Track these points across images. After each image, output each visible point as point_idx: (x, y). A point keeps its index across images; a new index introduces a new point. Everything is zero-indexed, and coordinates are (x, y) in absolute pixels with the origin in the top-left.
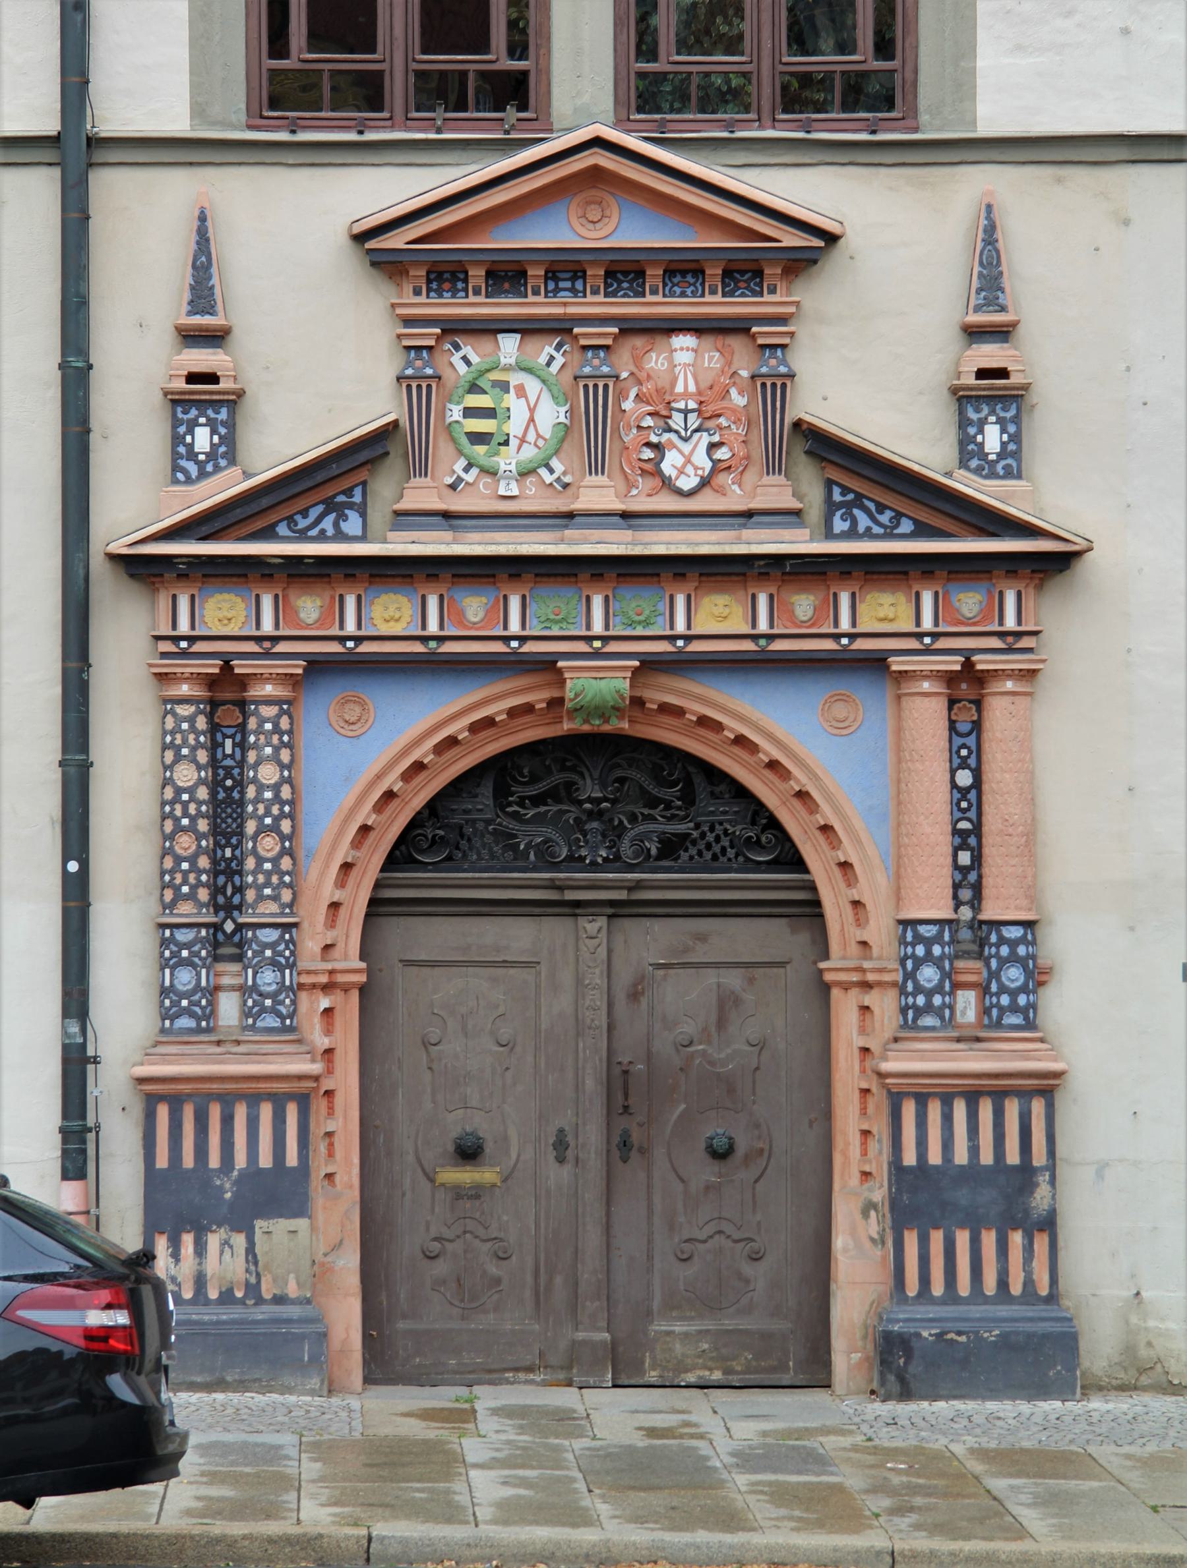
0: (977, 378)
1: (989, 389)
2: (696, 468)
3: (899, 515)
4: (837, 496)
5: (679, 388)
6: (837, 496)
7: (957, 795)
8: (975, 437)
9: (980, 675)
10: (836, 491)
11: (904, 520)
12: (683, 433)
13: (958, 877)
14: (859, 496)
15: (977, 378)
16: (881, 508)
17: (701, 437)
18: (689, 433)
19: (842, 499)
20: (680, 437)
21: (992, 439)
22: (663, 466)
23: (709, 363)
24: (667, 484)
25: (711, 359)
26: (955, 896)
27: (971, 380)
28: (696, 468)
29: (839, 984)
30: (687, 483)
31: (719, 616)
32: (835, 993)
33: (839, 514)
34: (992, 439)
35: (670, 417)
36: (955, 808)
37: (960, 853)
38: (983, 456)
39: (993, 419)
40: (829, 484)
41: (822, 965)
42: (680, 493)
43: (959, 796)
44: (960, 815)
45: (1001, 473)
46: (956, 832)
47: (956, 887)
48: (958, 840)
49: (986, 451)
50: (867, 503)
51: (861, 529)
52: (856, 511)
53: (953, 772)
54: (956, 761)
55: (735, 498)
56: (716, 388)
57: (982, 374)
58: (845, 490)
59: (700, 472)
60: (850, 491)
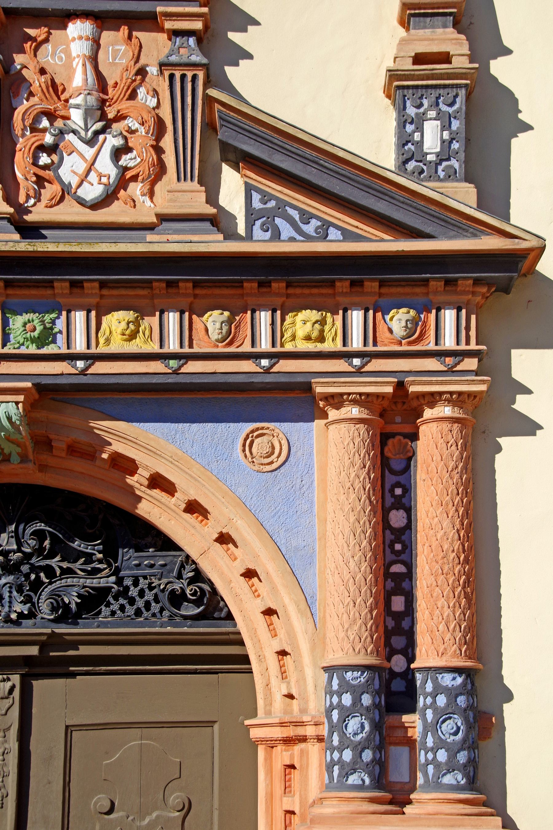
0: (414, 63)
1: (428, 78)
2: (100, 176)
3: (326, 225)
4: (257, 204)
5: (78, 81)
6: (257, 204)
7: (389, 536)
8: (411, 135)
9: (415, 403)
10: (256, 197)
11: (331, 230)
12: (83, 133)
13: (391, 623)
14: (282, 204)
15: (414, 63)
16: (306, 217)
17: (105, 139)
18: (90, 133)
19: (262, 206)
20: (81, 139)
21: (432, 137)
22: (62, 172)
23: (114, 59)
24: (66, 191)
25: (116, 53)
26: (387, 643)
27: (408, 65)
28: (100, 176)
29: (263, 741)
30: (92, 191)
31: (116, 334)
32: (261, 752)
33: (258, 223)
34: (432, 137)
35: (68, 118)
36: (388, 551)
37: (393, 598)
38: (422, 157)
39: (432, 114)
40: (249, 189)
41: (247, 722)
42: (81, 202)
43: (393, 537)
44: (393, 557)
45: (441, 174)
46: (387, 575)
47: (388, 634)
48: (390, 584)
49: (425, 150)
50: (291, 211)
51: (284, 236)
52: (278, 221)
53: (385, 512)
54: (389, 501)
55: (147, 211)
56: (121, 85)
57: (419, 59)
58: (266, 197)
59: (104, 180)
60: (272, 197)
